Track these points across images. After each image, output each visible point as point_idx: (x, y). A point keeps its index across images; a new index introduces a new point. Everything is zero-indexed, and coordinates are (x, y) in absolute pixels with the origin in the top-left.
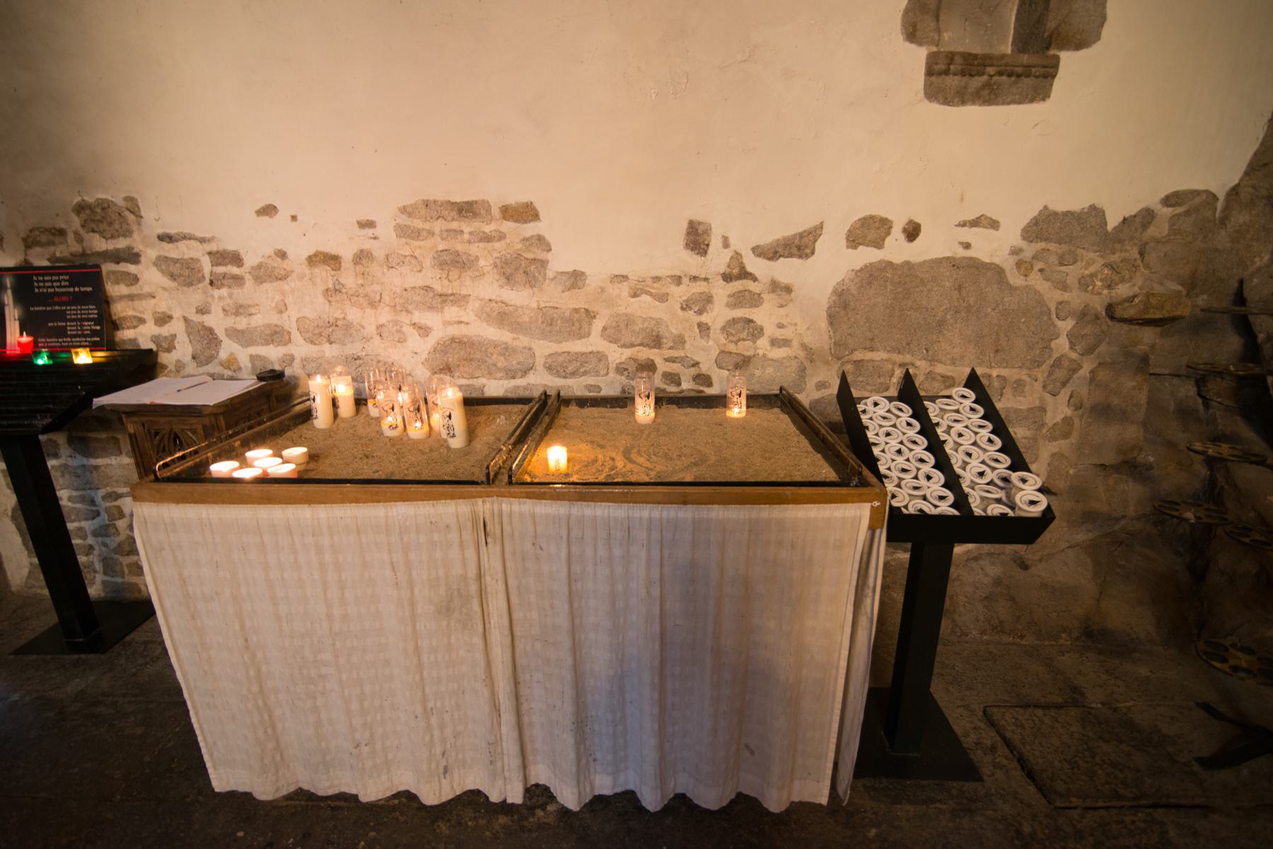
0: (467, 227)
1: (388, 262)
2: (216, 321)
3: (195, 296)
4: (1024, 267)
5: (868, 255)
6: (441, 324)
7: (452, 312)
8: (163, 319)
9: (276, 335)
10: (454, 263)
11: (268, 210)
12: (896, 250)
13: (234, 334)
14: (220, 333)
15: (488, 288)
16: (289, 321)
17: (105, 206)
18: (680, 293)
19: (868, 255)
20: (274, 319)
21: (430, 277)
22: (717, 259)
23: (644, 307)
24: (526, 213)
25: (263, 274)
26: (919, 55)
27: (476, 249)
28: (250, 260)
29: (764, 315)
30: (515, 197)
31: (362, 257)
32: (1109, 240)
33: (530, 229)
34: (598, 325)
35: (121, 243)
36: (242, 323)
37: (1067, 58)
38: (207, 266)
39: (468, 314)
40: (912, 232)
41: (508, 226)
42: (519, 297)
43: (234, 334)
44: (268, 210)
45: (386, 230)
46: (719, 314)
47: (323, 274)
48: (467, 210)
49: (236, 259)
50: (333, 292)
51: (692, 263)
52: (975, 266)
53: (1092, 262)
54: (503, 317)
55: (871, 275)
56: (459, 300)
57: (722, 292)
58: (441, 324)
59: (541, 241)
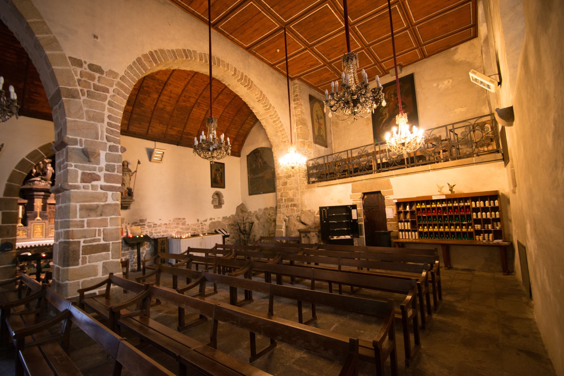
0: (179, 220)
1: (172, 224)
2: (153, 231)
3: (151, 229)
4: (223, 221)
5: (211, 221)
6: (176, 230)
7: (177, 229)
8: (147, 232)
9: (160, 232)
10: (178, 224)
11: (160, 220)
12: (213, 221)
13: (156, 233)
14: (153, 233)
15: (181, 226)
16: (161, 231)
17: (143, 220)
18: (197, 225)
19: (211, 221)
20: (160, 231)
21: (176, 225)
22: (200, 222)
23: (194, 227)
24: (184, 219)
25: (159, 226)
26: (213, 205)
27: (180, 222)
28: (158, 225)
29: (204, 227)
30: (183, 218)
31: (169, 224)
32: (228, 219)
33: (184, 220)
34: (190, 229)
35: (143, 223)
36: (156, 231)
37: (223, 205)
38: (153, 226)
39: (178, 229)
40: (214, 219)
41: (183, 220)
42: (183, 227)
43: (156, 233)
44: (160, 220)
45: (172, 221)
46: (200, 227)
47: (165, 226)
48: (179, 219)
49: (156, 224)
50: (166, 228)
51: (198, 222)
52: (219, 221)
53: (227, 221)
54: (182, 229)
55: (212, 223)
56: (178, 227)
57: (200, 225)
58: (176, 230)
59: (185, 221)
